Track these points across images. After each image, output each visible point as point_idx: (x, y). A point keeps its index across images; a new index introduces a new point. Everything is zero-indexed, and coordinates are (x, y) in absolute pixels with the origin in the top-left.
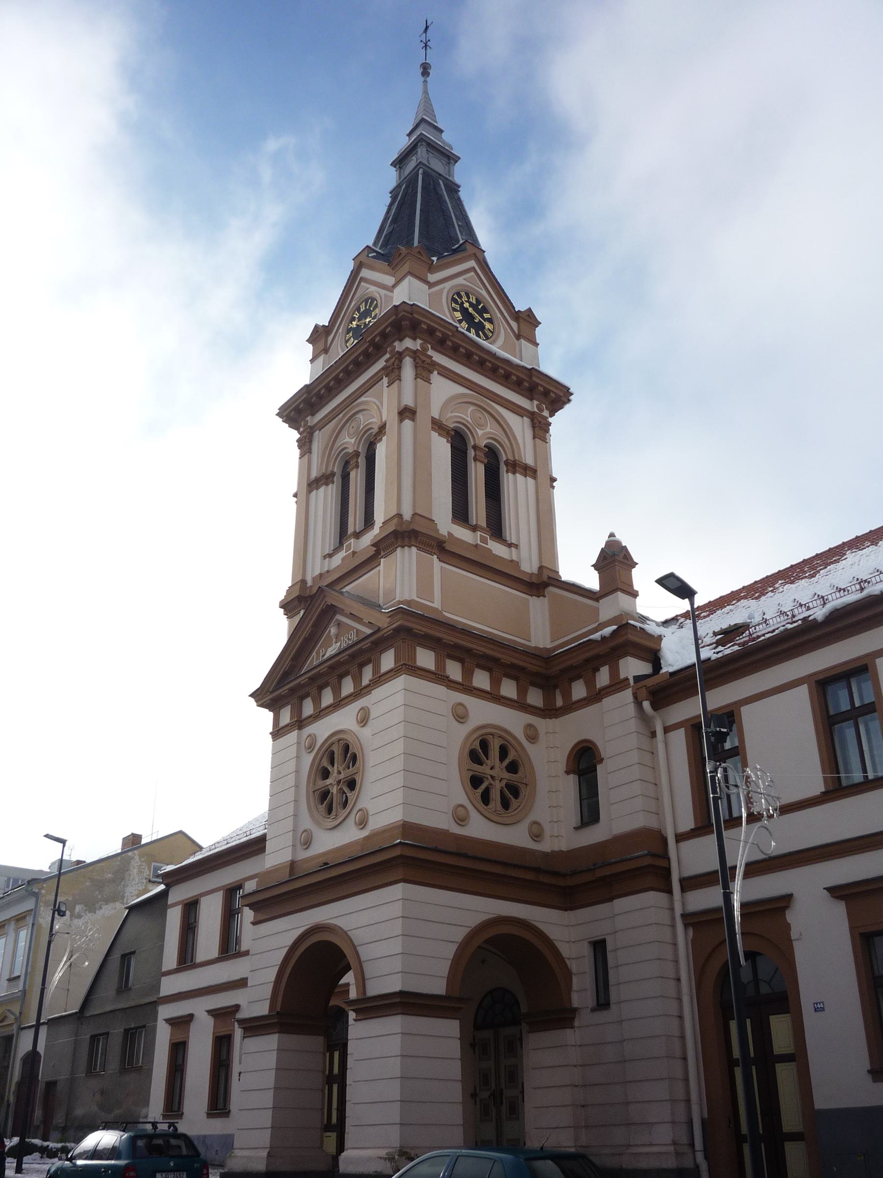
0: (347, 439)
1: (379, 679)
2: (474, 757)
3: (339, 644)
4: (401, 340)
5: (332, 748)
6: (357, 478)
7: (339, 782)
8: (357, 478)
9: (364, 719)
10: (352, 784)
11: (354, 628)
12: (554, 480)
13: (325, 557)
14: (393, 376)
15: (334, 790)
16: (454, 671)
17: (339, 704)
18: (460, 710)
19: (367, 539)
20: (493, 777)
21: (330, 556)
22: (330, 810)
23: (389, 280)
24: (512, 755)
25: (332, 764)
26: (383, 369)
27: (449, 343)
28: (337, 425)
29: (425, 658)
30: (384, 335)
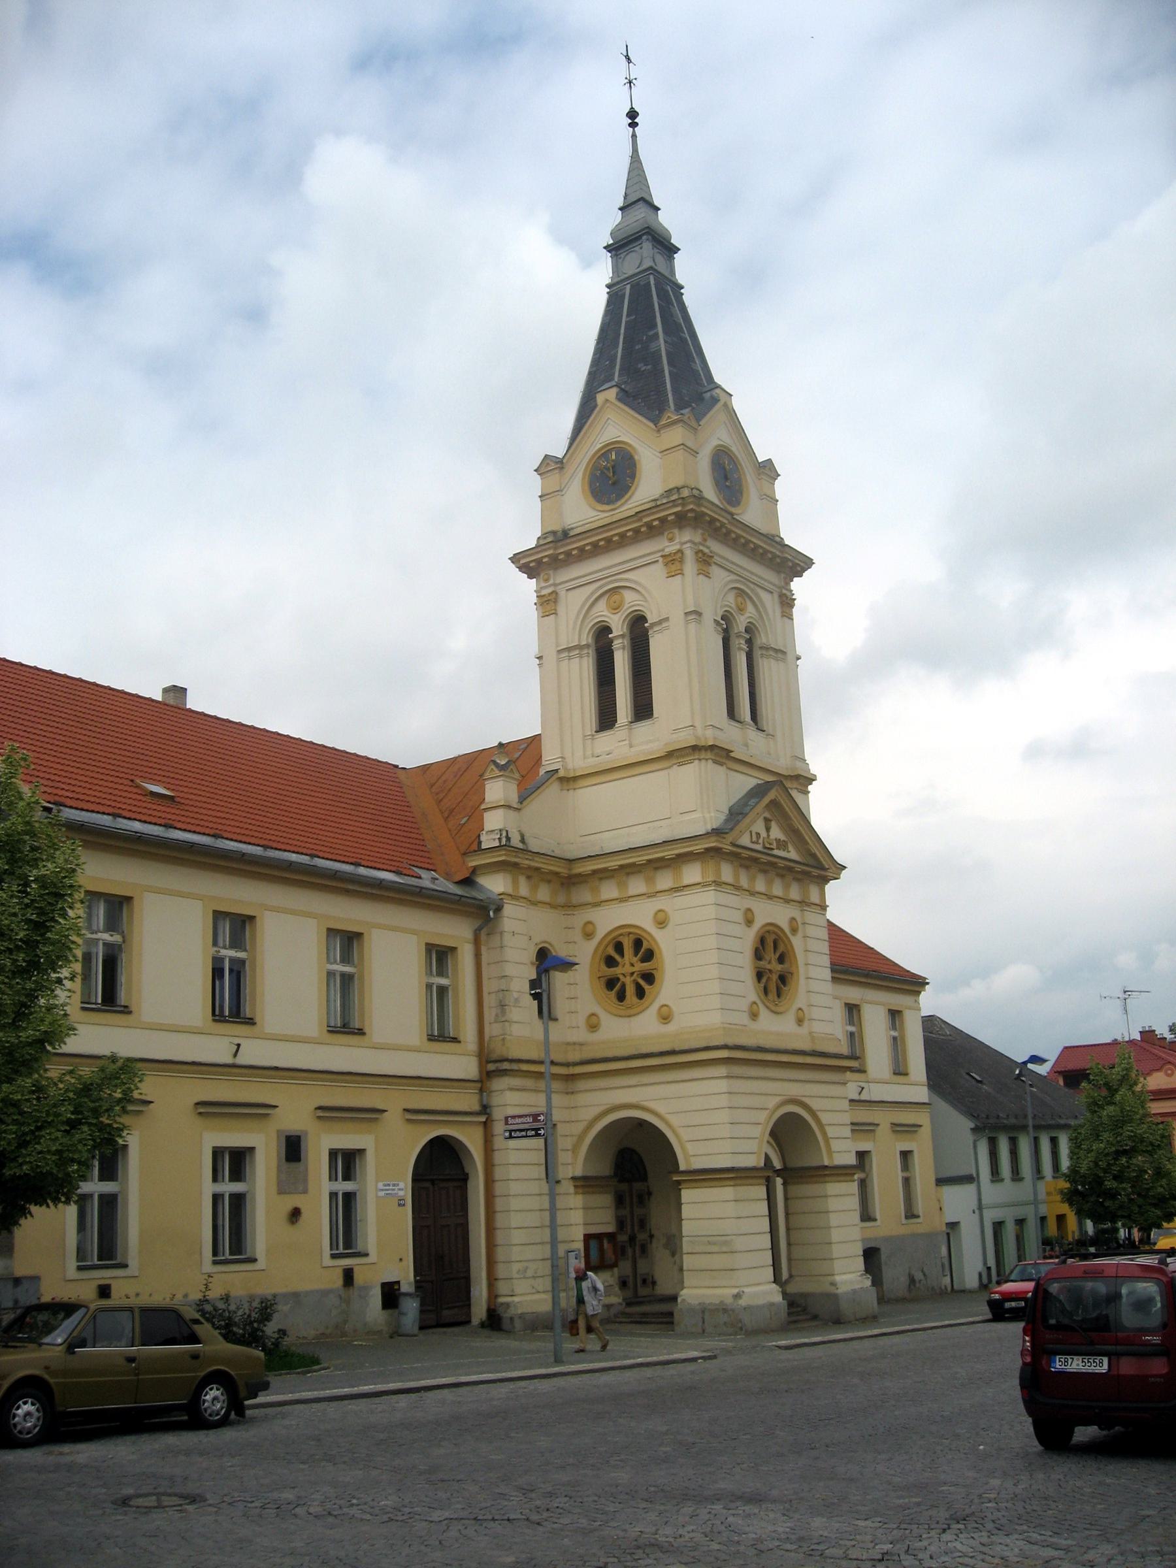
2: (758, 955)
5: (621, 939)
7: (632, 974)
10: (649, 978)
12: (798, 658)
14: (673, 568)
15: (629, 982)
16: (744, 882)
18: (749, 915)
20: (770, 971)
22: (621, 997)
24: (781, 949)
25: (622, 955)
27: (724, 530)
28: (592, 594)
29: (727, 872)
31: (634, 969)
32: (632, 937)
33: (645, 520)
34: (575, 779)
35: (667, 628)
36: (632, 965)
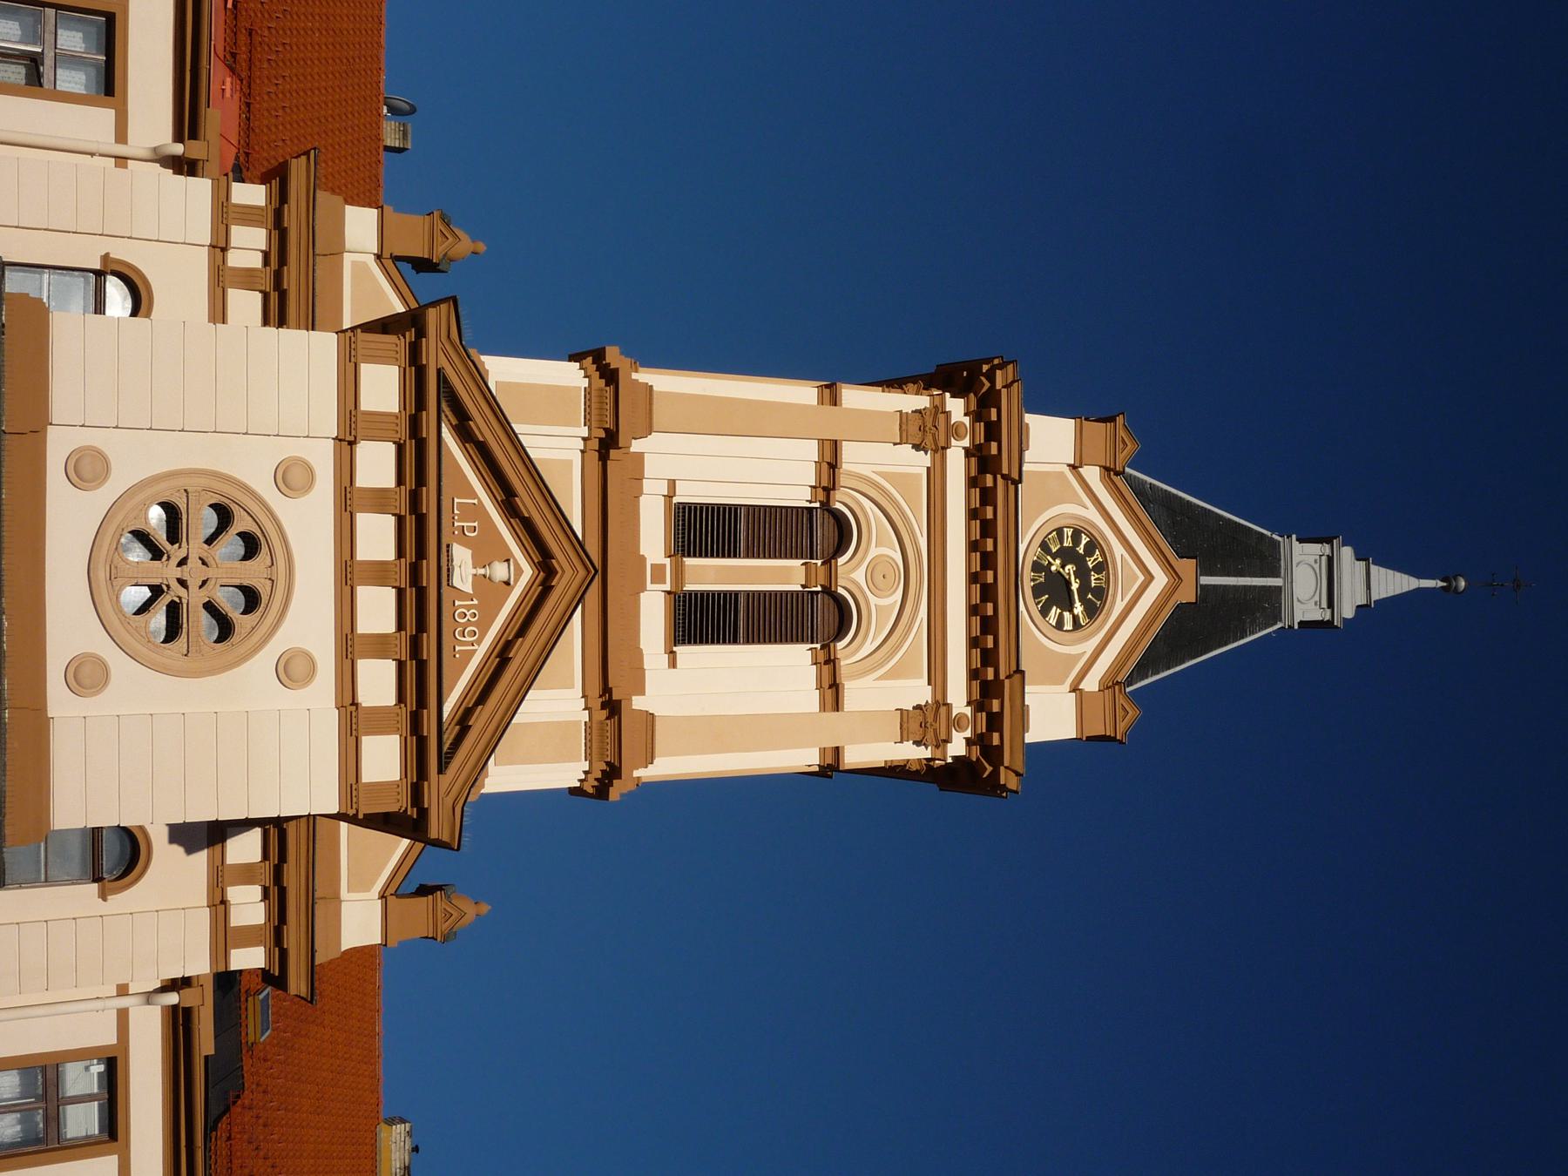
0: (874, 552)
1: (354, 720)
3: (467, 587)
4: (969, 742)
5: (263, 557)
6: (784, 575)
8: (784, 575)
9: (292, 671)
11: (479, 642)
13: (672, 484)
17: (349, 573)
19: (653, 612)
21: (669, 497)
23: (1091, 684)
26: (941, 703)
30: (995, 722)
31: (194, 584)
32: (263, 589)
33: (1007, 682)
34: (604, 458)
35: (823, 708)
36: (204, 583)
